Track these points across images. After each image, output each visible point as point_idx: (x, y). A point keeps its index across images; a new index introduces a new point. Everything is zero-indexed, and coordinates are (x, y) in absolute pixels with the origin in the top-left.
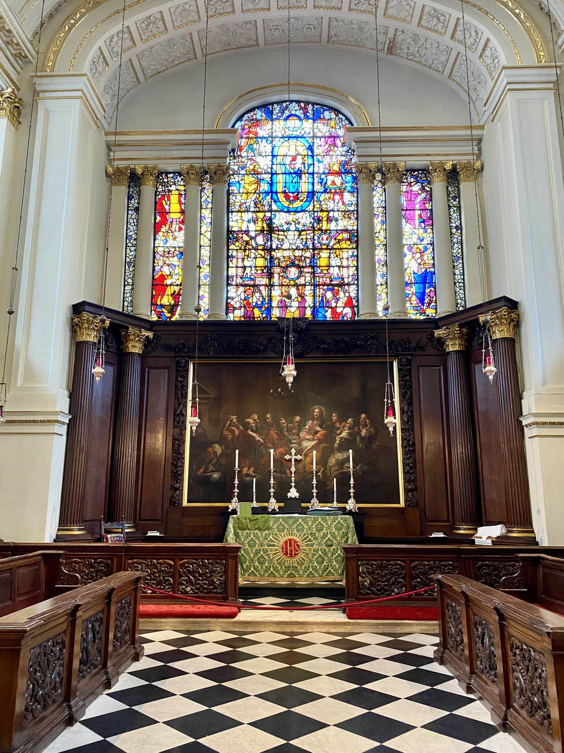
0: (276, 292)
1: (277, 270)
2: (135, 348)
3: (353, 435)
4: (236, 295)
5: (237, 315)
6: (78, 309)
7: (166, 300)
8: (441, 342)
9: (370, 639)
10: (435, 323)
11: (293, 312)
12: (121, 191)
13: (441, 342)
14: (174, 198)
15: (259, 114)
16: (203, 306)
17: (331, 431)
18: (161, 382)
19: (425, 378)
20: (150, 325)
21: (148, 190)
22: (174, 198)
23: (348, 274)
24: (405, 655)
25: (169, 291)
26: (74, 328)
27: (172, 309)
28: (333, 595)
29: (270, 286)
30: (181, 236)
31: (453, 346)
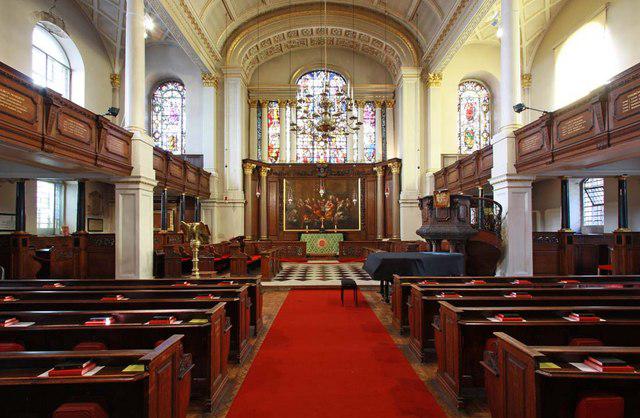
0: (315, 151)
1: (316, 143)
2: (264, 175)
3: (344, 206)
4: (301, 153)
5: (300, 161)
6: (244, 162)
7: (274, 155)
8: (376, 172)
9: (345, 266)
10: (374, 165)
11: (322, 160)
12: (254, 110)
13: (376, 172)
14: (275, 113)
15: (308, 76)
16: (287, 158)
17: (336, 204)
18: (274, 186)
19: (369, 185)
20: (269, 165)
21: (265, 110)
22: (275, 113)
23: (343, 145)
24: (356, 271)
25: (275, 151)
26: (243, 168)
27: (276, 158)
28: (335, 257)
29: (313, 149)
30: (278, 129)
31: (379, 175)
